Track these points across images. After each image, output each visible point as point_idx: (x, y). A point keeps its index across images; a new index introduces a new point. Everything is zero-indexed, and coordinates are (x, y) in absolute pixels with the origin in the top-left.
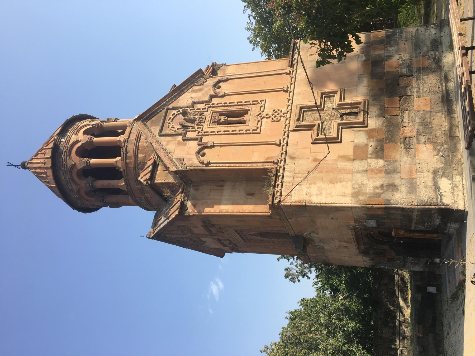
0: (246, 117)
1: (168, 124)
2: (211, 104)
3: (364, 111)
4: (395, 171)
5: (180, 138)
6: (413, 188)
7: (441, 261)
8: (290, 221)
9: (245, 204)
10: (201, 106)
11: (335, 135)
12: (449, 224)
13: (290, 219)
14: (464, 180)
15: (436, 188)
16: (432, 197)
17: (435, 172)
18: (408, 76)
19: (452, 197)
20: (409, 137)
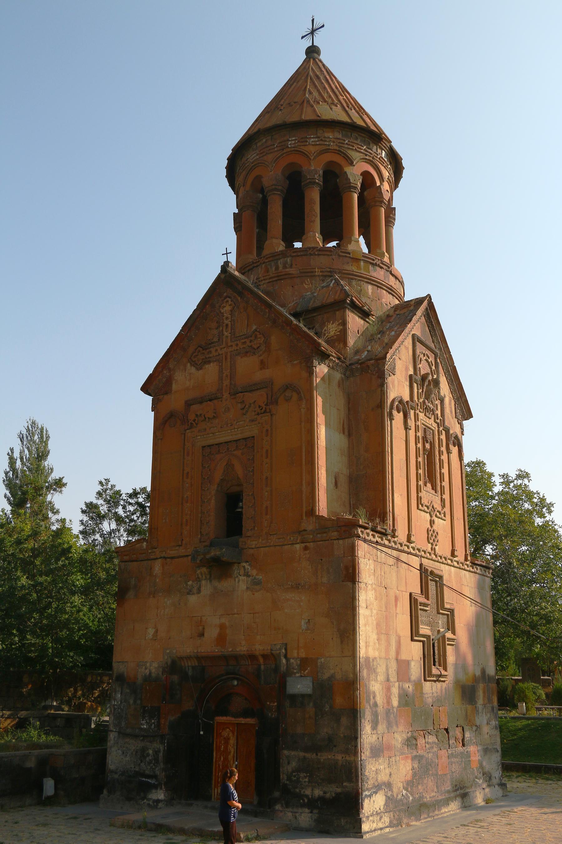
0: (429, 485)
1: (424, 352)
2: (441, 429)
3: (441, 676)
4: (389, 725)
5: (411, 372)
6: (377, 752)
7: (158, 801)
8: (298, 546)
9: (327, 471)
10: (439, 412)
11: (422, 632)
12: (307, 810)
13: (306, 548)
14: (387, 830)
15: (378, 788)
16: (369, 783)
17: (389, 785)
18: (463, 740)
19: (369, 813)
20: (417, 745)
